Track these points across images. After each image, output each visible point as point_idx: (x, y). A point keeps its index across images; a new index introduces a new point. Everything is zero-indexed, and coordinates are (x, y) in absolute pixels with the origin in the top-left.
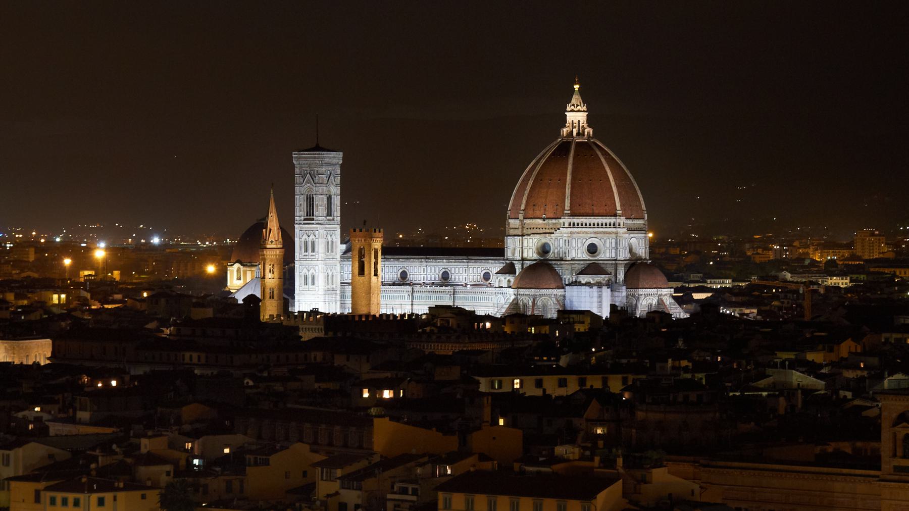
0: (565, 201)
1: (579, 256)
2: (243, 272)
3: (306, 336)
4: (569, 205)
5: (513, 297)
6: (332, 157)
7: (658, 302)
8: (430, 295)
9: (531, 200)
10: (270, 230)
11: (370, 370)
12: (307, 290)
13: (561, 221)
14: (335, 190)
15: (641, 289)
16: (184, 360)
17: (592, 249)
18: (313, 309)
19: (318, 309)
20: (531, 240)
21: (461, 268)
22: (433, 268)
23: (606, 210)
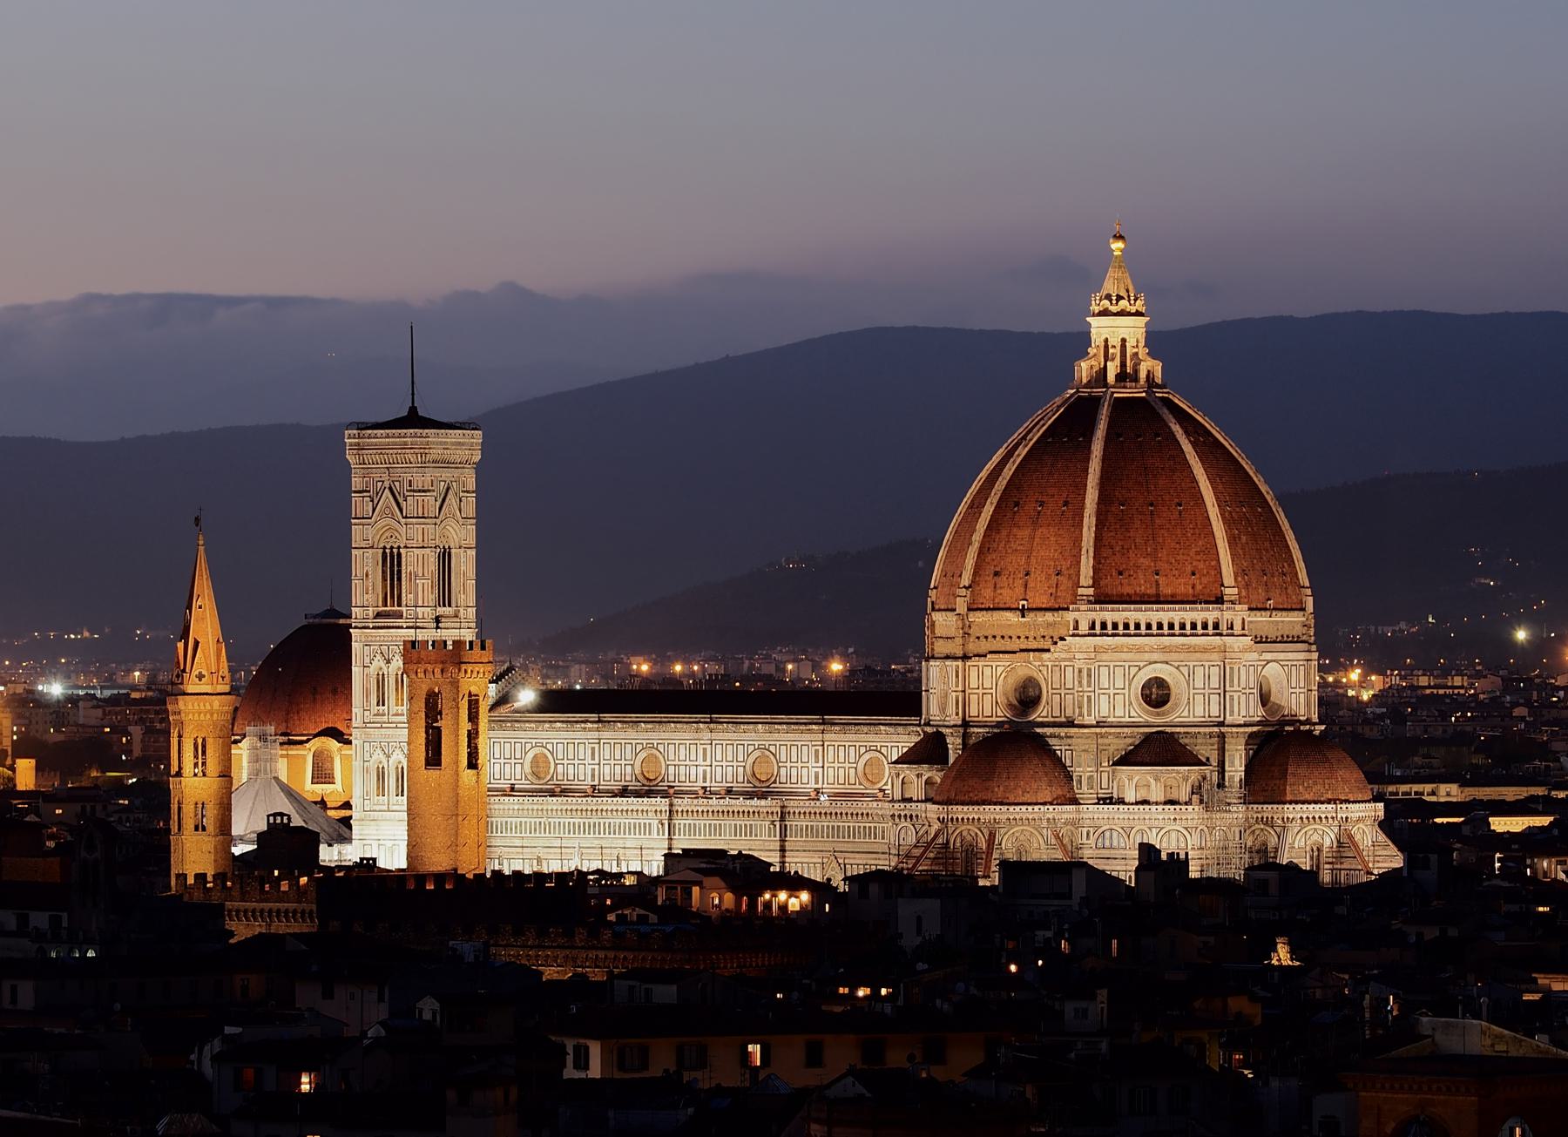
0: (1079, 563)
1: (1119, 712)
5: (936, 826)
6: (452, 444)
7: (1339, 841)
10: (197, 643)
12: (385, 808)
13: (1070, 616)
14: (461, 535)
15: (1291, 802)
17: (1156, 694)
18: (362, 859)
19: (374, 860)
21: (805, 748)
22: (730, 747)
23: (1193, 588)
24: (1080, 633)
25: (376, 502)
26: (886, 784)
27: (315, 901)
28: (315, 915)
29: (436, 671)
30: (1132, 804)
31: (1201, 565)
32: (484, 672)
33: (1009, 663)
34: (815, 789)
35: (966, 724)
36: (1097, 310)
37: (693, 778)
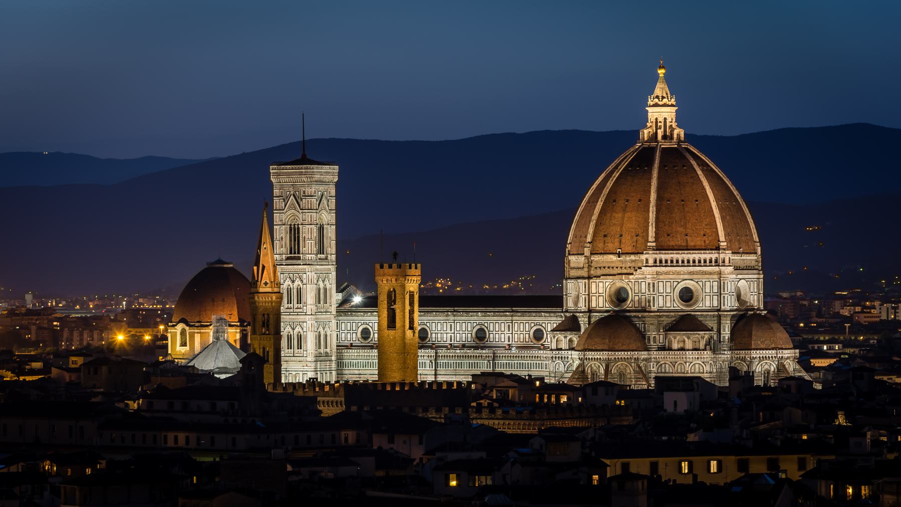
1: (668, 305)
2: (189, 334)
3: (328, 411)
4: (654, 235)
5: (577, 362)
6: (325, 172)
7: (778, 368)
8: (460, 361)
9: (601, 229)
10: (264, 267)
11: (423, 455)
12: (292, 355)
13: (643, 257)
14: (328, 217)
15: (754, 349)
16: (166, 442)
17: (687, 296)
18: (310, 379)
20: (601, 284)
21: (503, 324)
22: (464, 324)
23: (704, 242)
24: (649, 265)
25: (286, 201)
26: (545, 342)
27: (343, 396)
28: (343, 403)
29: (393, 280)
30: (676, 350)
31: (708, 231)
32: (416, 280)
33: (612, 281)
34: (508, 345)
35: (590, 311)
36: (652, 104)
37: (445, 340)
